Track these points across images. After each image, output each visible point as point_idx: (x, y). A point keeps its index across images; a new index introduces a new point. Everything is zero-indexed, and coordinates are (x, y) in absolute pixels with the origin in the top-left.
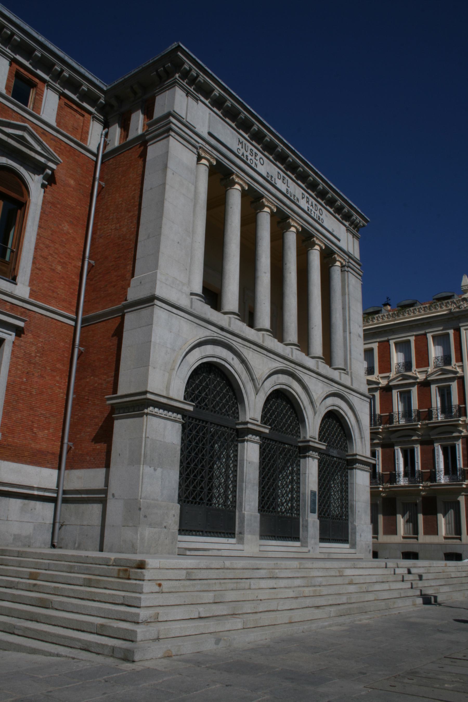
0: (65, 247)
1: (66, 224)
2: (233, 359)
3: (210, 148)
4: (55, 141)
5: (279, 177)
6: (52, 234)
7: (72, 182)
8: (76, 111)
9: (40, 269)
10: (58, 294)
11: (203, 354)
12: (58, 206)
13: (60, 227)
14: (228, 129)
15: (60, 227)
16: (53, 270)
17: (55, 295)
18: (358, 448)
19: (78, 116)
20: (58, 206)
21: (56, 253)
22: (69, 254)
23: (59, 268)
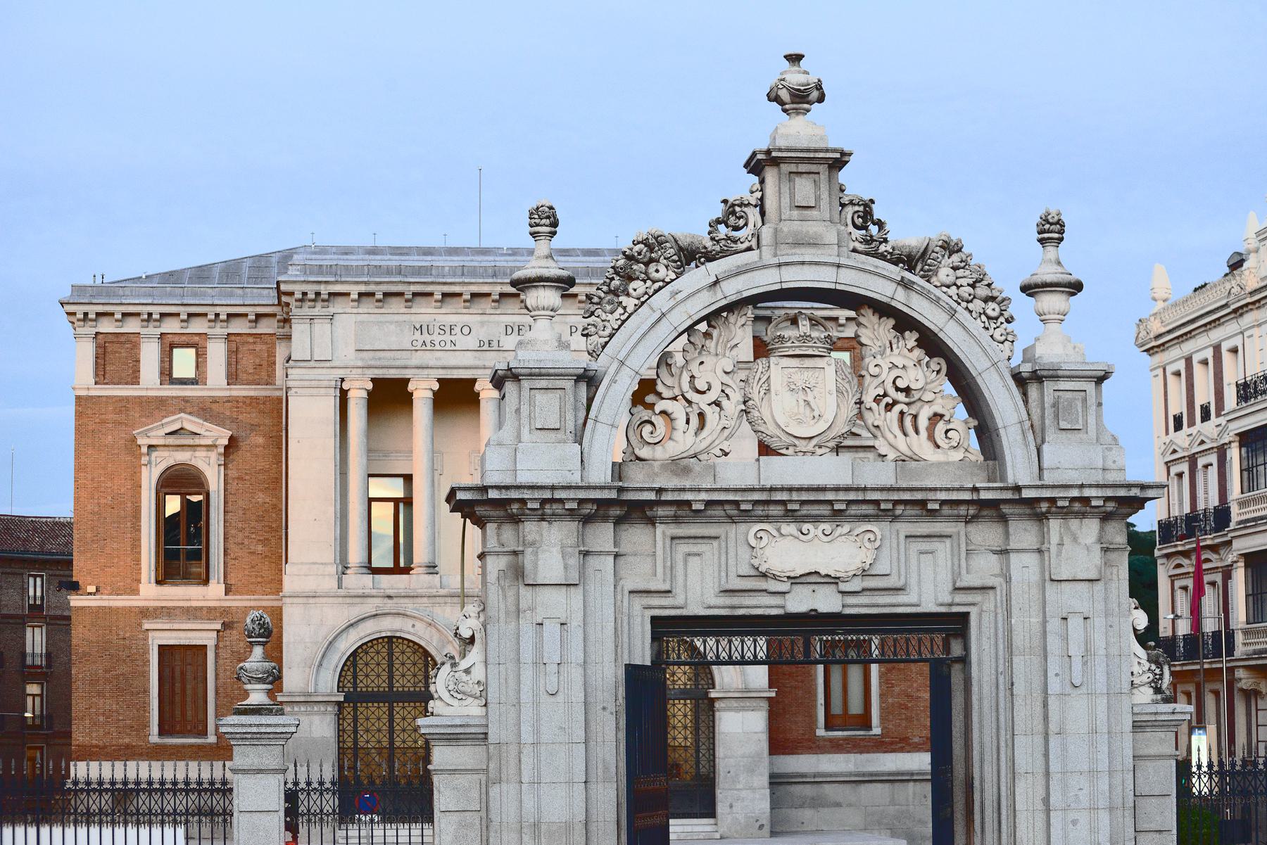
0: (262, 521)
1: (261, 495)
2: (413, 626)
3: (360, 371)
4: (229, 401)
5: (509, 332)
6: (244, 514)
7: (261, 440)
8: (255, 343)
9: (235, 559)
10: (263, 577)
11: (362, 634)
12: (247, 477)
13: (253, 500)
14: (391, 323)
15: (253, 500)
16: (253, 553)
17: (259, 580)
18: (726, 680)
19: (258, 347)
20: (247, 477)
21: (253, 533)
22: (271, 527)
23: (260, 548)
